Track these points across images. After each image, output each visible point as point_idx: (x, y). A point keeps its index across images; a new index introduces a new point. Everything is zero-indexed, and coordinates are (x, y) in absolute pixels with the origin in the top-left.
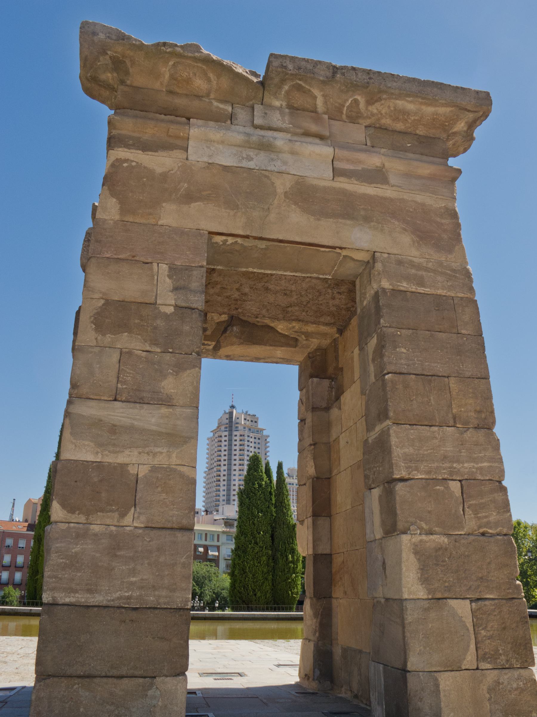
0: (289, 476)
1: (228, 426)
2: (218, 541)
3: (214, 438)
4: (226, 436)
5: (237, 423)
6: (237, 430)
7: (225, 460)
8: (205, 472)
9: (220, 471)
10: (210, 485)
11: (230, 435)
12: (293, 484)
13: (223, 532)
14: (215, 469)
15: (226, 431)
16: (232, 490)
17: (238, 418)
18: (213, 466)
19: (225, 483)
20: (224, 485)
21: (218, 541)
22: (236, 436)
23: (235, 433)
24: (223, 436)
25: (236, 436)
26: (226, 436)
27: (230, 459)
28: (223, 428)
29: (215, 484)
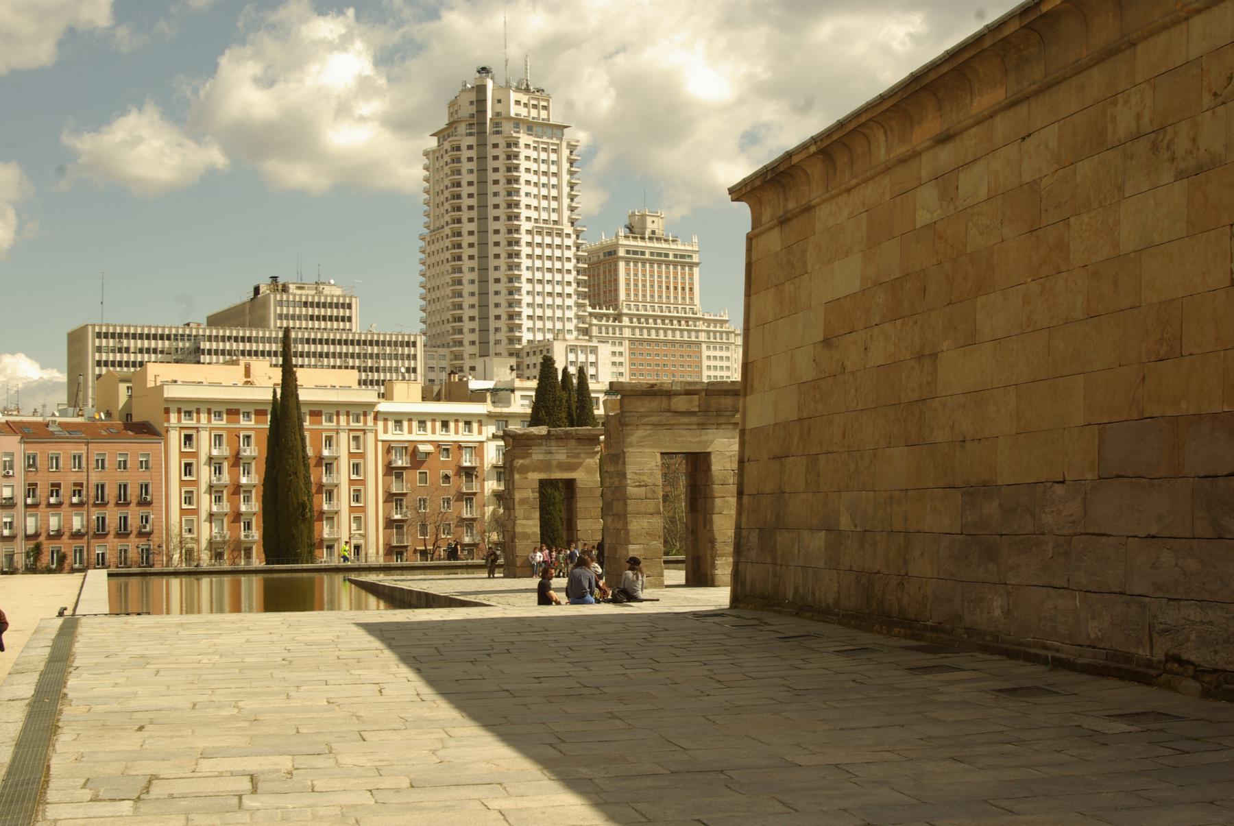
0: (631, 232)
1: (475, 121)
2: (480, 433)
3: (443, 152)
4: (470, 147)
5: (498, 114)
6: (498, 133)
7: (471, 208)
8: (423, 239)
9: (459, 234)
10: (438, 269)
11: (482, 144)
12: (643, 253)
13: (490, 416)
14: (447, 230)
15: (471, 134)
16: (491, 281)
17: (499, 101)
18: (443, 222)
19: (474, 263)
20: (472, 269)
21: (480, 433)
22: (496, 146)
23: (492, 139)
24: (464, 147)
25: (496, 146)
26: (470, 147)
27: (483, 206)
28: (462, 129)
29: (448, 267)
